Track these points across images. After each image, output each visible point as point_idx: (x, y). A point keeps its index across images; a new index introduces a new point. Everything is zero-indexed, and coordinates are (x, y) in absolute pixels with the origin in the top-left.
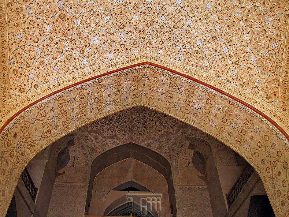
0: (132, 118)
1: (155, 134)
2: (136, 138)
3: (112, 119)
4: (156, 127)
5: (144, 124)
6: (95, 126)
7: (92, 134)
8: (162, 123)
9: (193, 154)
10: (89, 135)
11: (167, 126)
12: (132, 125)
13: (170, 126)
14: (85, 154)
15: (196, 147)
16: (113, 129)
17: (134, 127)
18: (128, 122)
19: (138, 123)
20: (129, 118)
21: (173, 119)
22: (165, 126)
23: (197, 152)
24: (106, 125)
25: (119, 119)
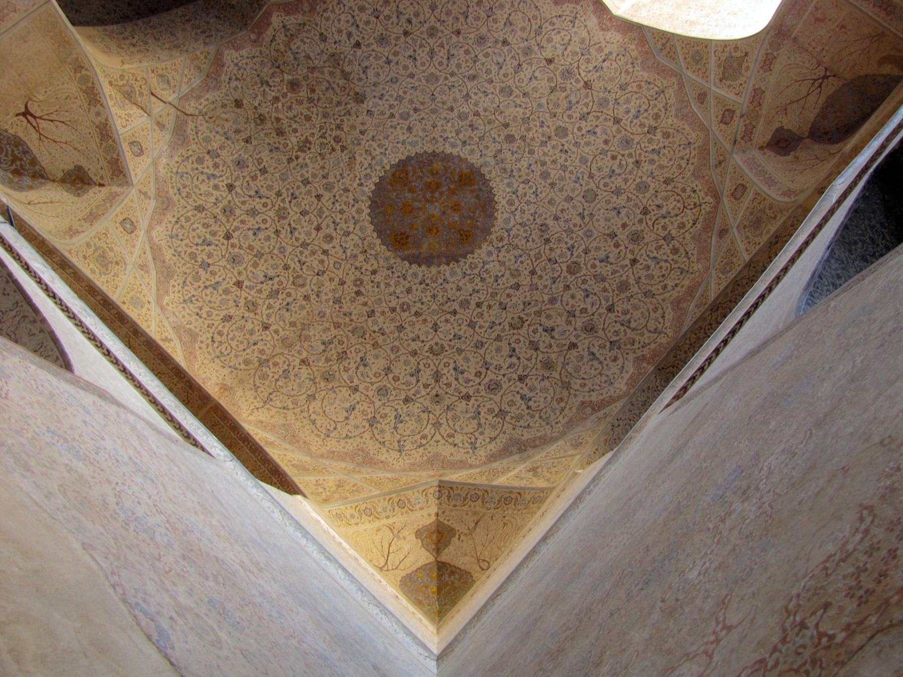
0: (303, 330)
1: (318, 436)
2: (243, 399)
3: (247, 283)
4: (347, 418)
5: (317, 381)
6: (179, 249)
7: (148, 248)
8: (378, 416)
9: (419, 564)
10: (141, 234)
11: (388, 436)
12: (278, 350)
13: (399, 442)
14: (72, 232)
15: (455, 540)
16: (209, 314)
17: (276, 364)
18: (276, 332)
19: (303, 361)
20: (293, 324)
21: (430, 426)
22: (382, 431)
23: (439, 569)
24: (208, 283)
25: (260, 302)
